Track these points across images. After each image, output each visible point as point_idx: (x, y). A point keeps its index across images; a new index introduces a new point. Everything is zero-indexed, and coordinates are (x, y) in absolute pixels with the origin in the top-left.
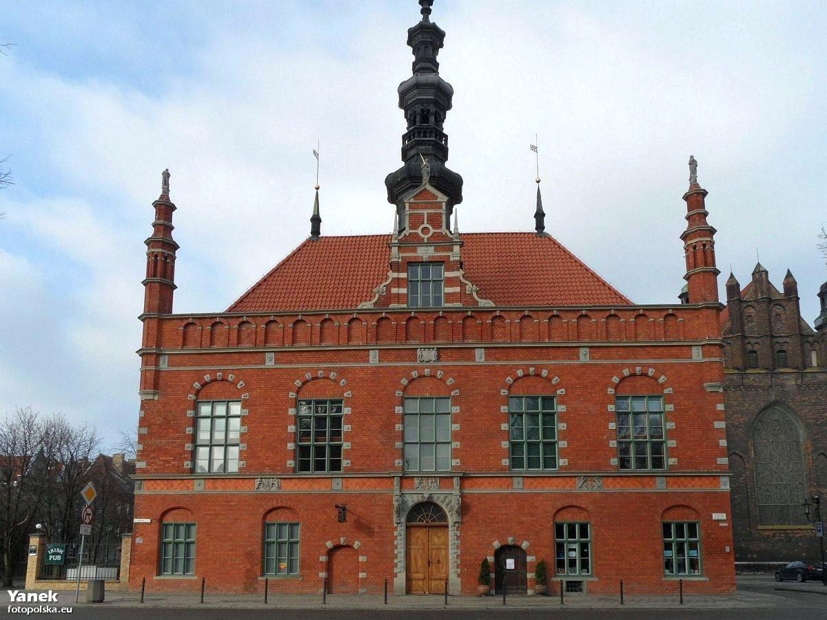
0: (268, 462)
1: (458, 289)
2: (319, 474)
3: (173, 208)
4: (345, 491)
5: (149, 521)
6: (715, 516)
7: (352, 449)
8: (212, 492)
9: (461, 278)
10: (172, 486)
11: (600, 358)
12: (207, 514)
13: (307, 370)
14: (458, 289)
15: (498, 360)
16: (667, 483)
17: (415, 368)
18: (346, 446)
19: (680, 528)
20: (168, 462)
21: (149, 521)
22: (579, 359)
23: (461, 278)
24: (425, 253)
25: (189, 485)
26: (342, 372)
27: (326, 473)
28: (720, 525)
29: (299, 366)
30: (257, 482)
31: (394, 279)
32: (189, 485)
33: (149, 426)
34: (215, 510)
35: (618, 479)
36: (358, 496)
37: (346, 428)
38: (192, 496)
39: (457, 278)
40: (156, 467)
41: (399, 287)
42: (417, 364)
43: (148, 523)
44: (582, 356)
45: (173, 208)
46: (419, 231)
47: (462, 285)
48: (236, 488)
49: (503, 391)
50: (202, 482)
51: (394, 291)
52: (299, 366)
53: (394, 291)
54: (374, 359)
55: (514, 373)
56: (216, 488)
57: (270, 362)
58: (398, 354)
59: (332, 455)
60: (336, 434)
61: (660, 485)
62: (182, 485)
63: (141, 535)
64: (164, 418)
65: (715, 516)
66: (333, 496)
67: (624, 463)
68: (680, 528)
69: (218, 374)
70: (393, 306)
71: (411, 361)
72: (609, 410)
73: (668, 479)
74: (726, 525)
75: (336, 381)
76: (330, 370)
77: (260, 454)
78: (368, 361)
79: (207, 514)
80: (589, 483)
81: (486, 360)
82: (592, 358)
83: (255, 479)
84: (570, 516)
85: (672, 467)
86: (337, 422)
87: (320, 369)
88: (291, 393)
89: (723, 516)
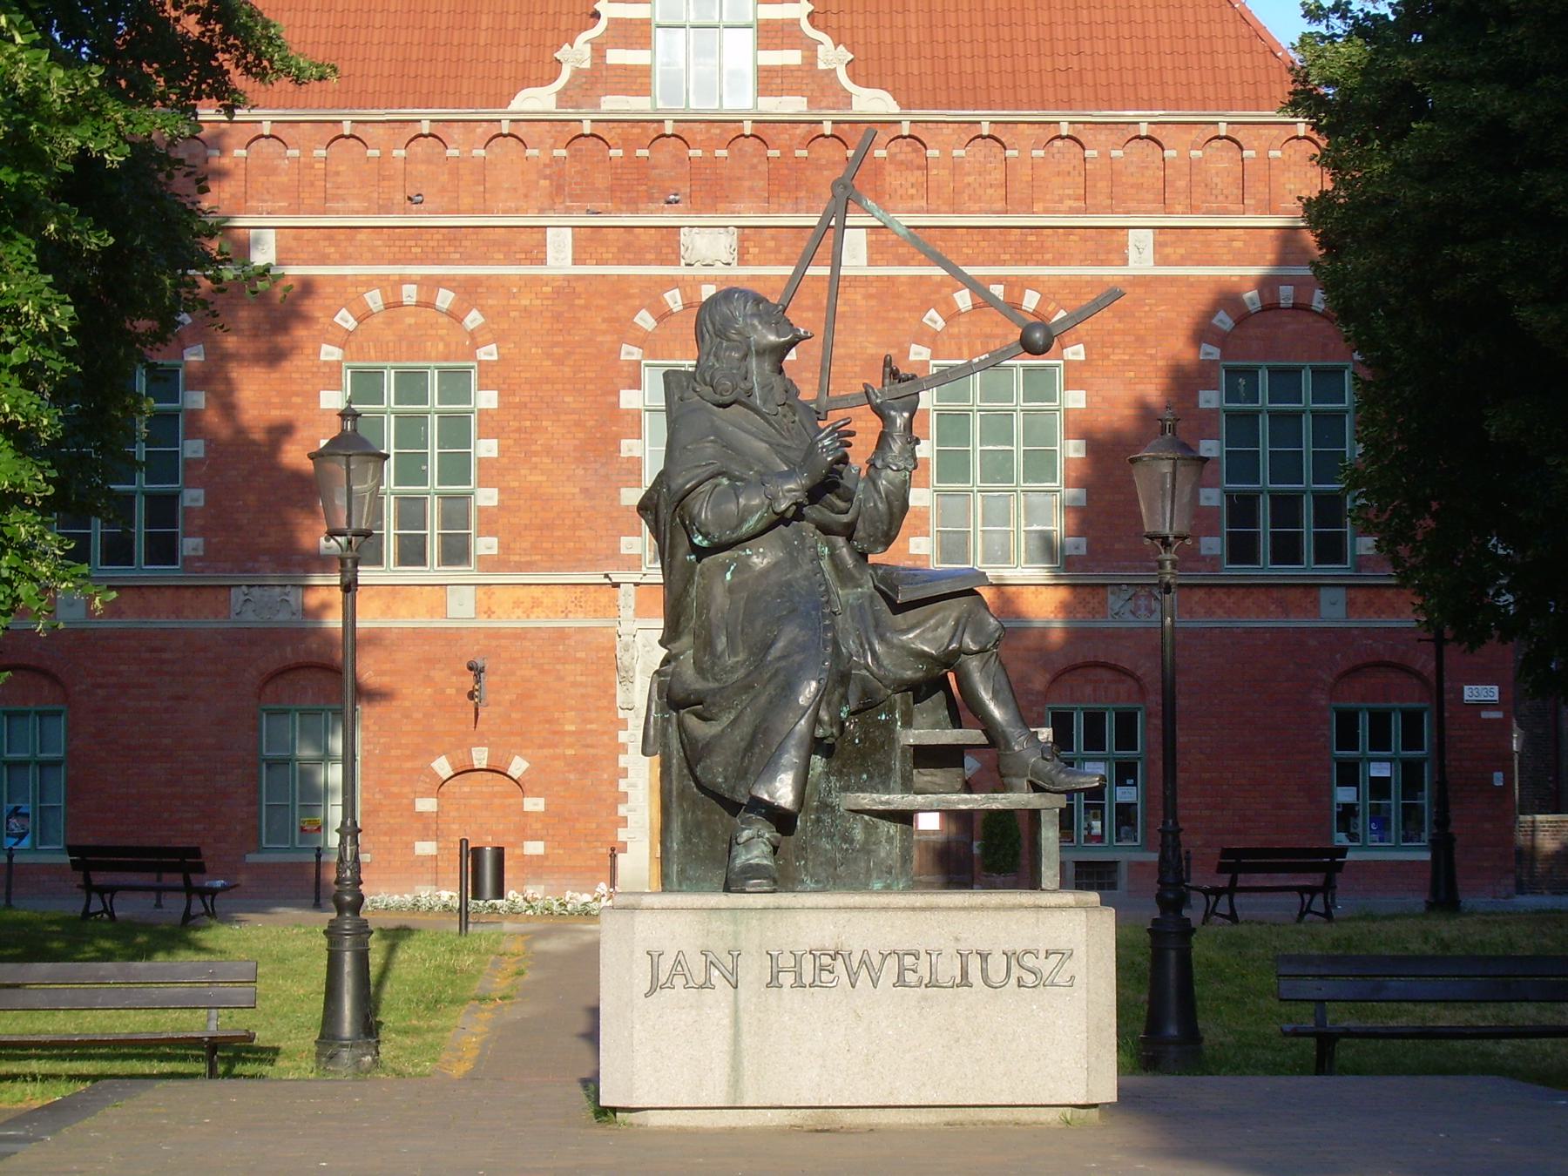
1: (793, 57)
2: (411, 575)
4: (483, 623)
6: (1472, 693)
7: (502, 507)
9: (805, 25)
11: (1182, 262)
12: (100, 686)
13: (370, 283)
14: (793, 57)
15: (904, 263)
16: (1351, 604)
17: (673, 282)
18: (486, 497)
19: (1380, 723)
22: (1125, 262)
23: (805, 25)
26: (469, 290)
27: (433, 572)
28: (1485, 715)
30: (237, 596)
31: (614, 22)
35: (1220, 593)
36: (520, 635)
37: (485, 448)
39: (796, 22)
41: (629, 46)
44: (1132, 254)
47: (811, 47)
49: (914, 348)
51: (615, 57)
53: (615, 57)
54: (560, 257)
55: (950, 302)
58: (630, 246)
59: (446, 521)
60: (456, 468)
61: (1332, 611)
65: (1472, 693)
66: (449, 637)
67: (1242, 549)
68: (1380, 723)
70: (614, 104)
71: (663, 262)
72: (1202, 405)
73: (1353, 593)
74: (1497, 715)
75: (455, 316)
78: (543, 262)
79: (100, 686)
80: (1142, 602)
81: (872, 262)
82: (1161, 260)
84: (1088, 690)
85: (1361, 562)
86: (456, 429)
87: (404, 280)
88: (325, 348)
89: (1491, 693)
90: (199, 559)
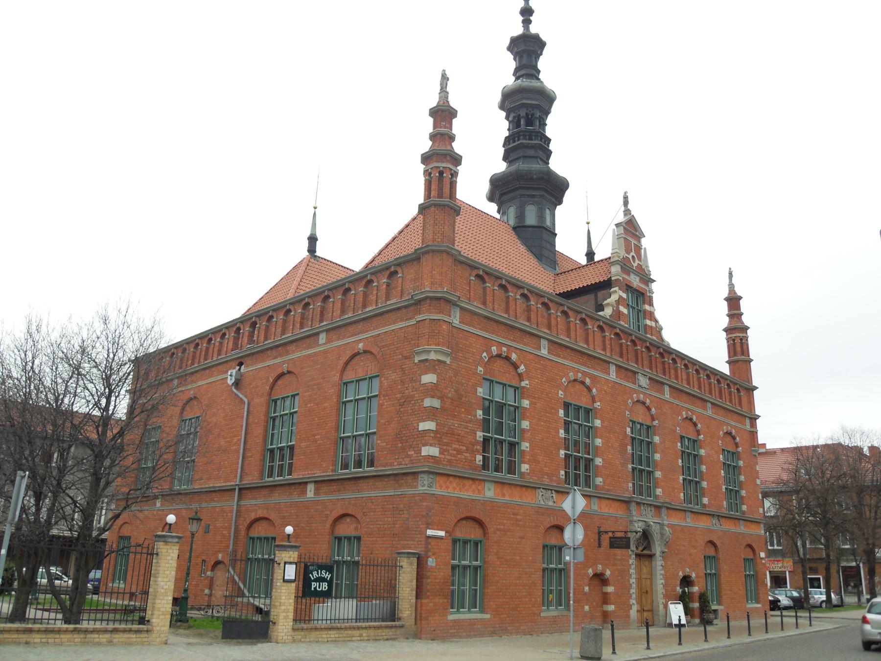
0: (546, 470)
3: (453, 113)
5: (442, 533)
8: (501, 499)
10: (464, 486)
20: (459, 452)
21: (442, 533)
24: (635, 281)
25: (480, 488)
29: (566, 362)
30: (540, 493)
32: (480, 488)
33: (442, 398)
34: (504, 524)
38: (484, 503)
40: (449, 457)
42: (636, 387)
43: (441, 538)
45: (453, 113)
46: (630, 257)
48: (521, 497)
50: (491, 486)
52: (566, 362)
56: (504, 495)
57: (544, 352)
62: (474, 487)
63: (433, 554)
64: (456, 391)
69: (504, 349)
76: (585, 374)
77: (540, 458)
83: (536, 488)
87: (579, 371)
90: (528, 474)
